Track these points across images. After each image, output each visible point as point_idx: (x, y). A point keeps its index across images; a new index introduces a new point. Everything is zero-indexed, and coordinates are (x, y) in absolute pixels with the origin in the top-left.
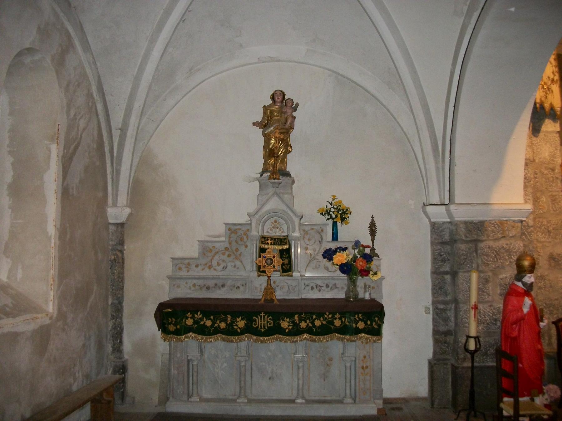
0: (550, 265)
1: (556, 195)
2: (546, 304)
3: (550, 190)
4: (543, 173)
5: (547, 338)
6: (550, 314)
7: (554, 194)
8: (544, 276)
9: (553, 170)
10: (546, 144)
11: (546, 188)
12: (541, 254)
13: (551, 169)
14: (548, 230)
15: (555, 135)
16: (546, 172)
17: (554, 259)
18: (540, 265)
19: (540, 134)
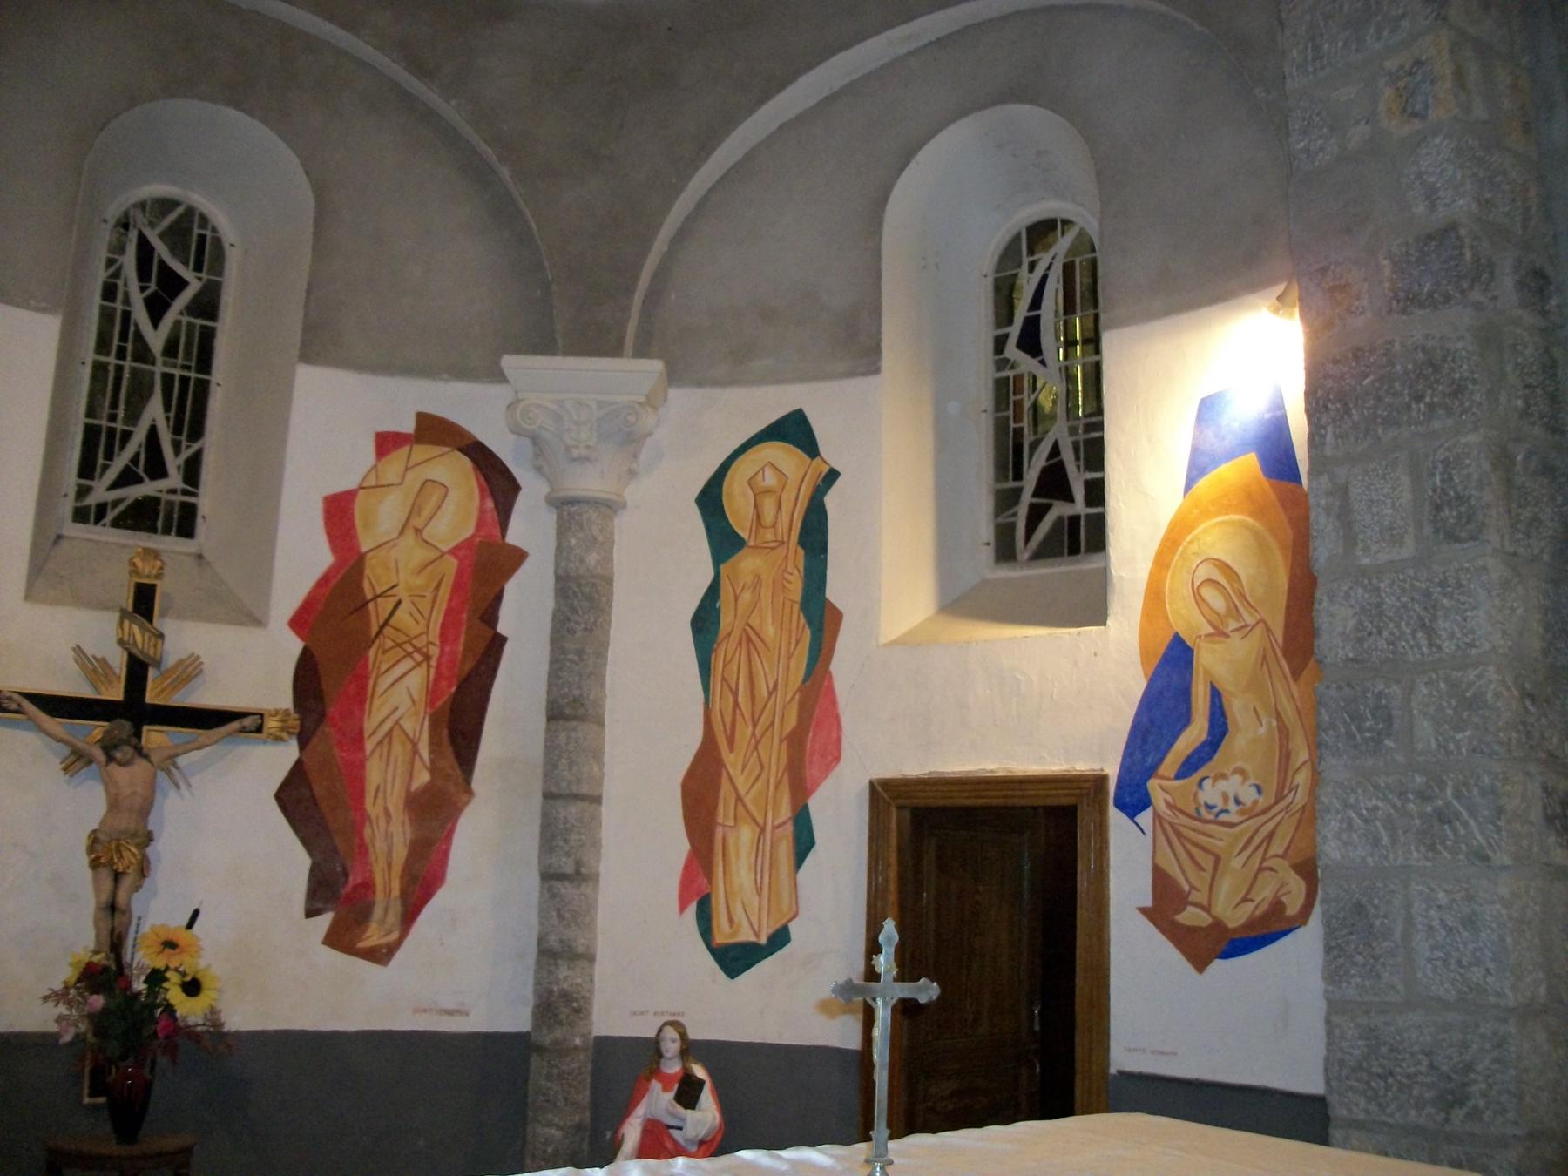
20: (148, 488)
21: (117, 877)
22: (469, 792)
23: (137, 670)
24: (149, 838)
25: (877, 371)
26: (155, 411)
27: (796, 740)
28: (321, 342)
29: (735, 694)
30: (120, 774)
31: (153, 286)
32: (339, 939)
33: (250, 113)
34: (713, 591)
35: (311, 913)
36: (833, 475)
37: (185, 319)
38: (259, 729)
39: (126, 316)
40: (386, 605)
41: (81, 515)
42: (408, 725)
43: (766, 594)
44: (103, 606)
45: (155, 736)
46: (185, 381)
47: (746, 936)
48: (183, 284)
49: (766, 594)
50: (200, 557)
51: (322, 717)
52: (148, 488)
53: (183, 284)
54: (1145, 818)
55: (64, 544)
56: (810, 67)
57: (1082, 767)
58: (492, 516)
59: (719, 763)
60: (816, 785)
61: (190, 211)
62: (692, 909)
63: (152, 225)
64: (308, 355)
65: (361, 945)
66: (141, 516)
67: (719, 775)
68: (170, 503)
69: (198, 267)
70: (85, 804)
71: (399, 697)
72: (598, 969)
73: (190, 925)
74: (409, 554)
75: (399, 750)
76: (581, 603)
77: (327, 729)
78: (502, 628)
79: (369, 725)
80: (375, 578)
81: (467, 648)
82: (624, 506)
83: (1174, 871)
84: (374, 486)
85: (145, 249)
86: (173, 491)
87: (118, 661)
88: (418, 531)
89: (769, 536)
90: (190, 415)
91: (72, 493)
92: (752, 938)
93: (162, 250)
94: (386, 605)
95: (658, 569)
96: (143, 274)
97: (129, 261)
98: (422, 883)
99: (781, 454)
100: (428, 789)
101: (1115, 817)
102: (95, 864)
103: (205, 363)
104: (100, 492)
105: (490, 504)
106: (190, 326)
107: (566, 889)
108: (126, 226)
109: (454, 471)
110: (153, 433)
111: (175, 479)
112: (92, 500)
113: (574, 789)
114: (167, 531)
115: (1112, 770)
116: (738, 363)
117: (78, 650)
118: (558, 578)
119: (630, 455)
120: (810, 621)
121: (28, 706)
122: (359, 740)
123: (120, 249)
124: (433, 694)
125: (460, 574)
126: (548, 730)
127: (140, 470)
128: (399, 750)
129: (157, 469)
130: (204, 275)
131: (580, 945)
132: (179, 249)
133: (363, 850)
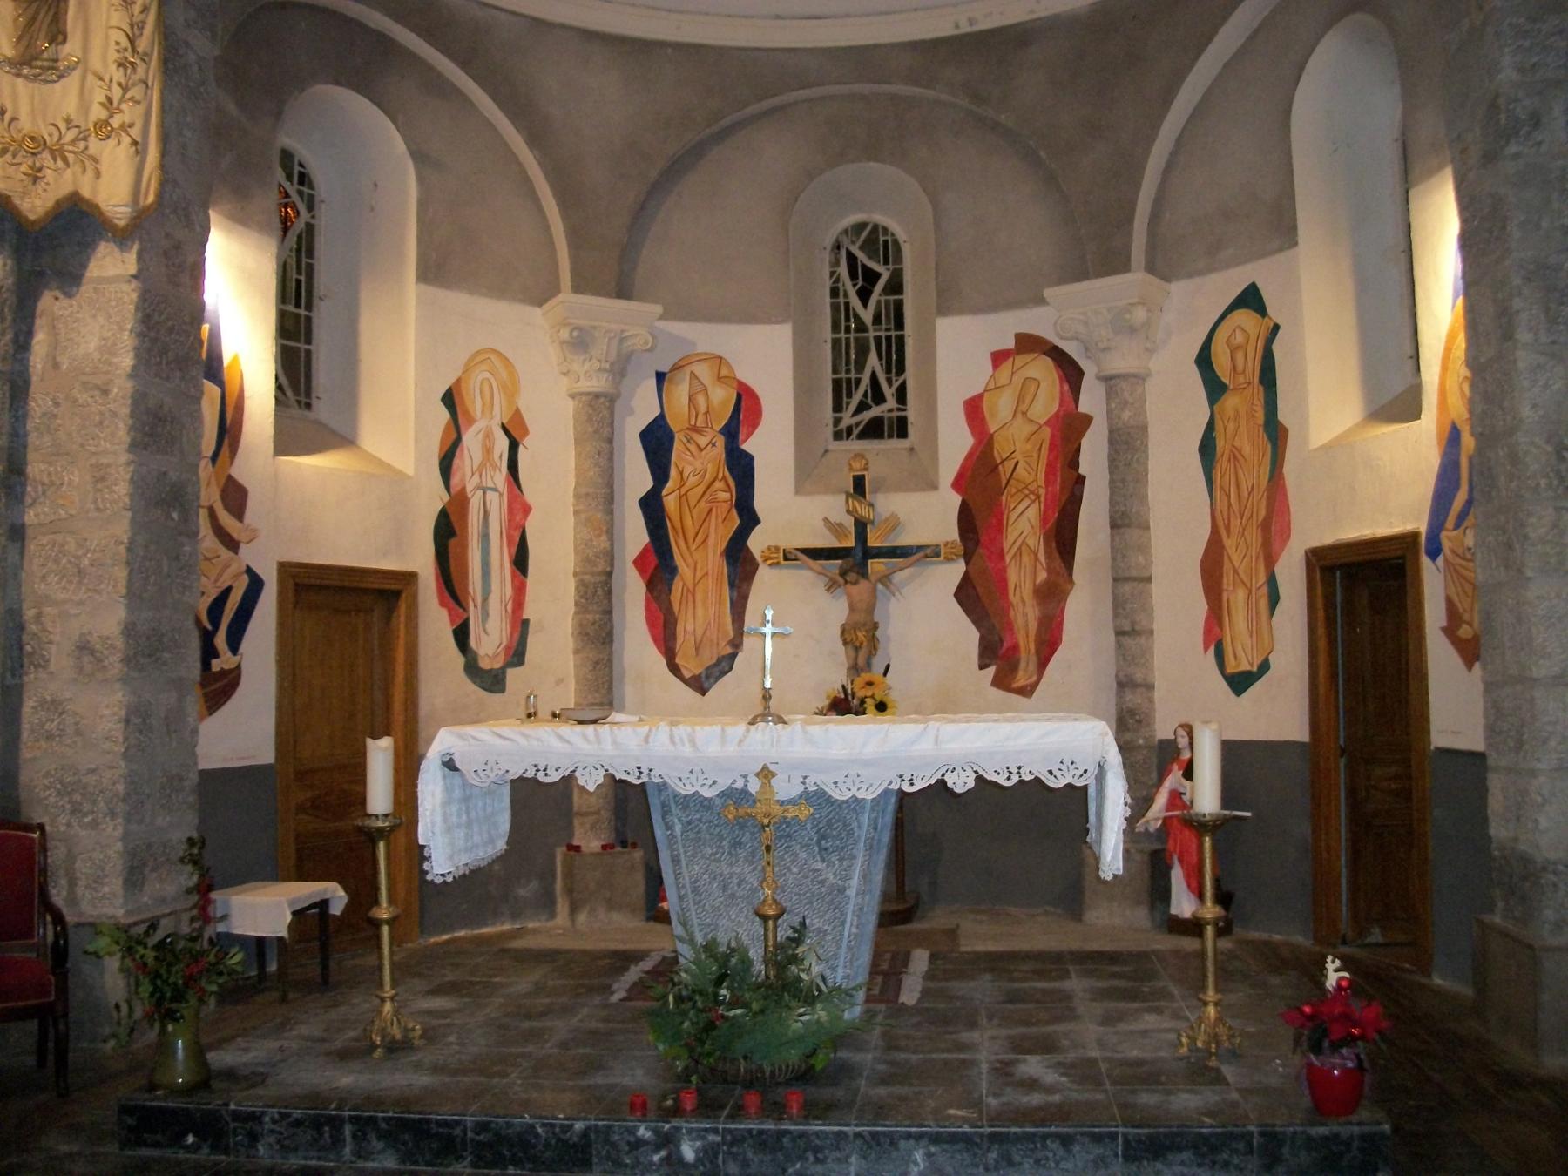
0: (81, 669)
1: (108, 465)
2: (61, 783)
3: (93, 449)
4: (75, 401)
5: (63, 882)
6: (73, 812)
7: (105, 461)
8: (61, 703)
9: (105, 392)
10: (94, 316)
11: (82, 445)
12: (57, 638)
13: (98, 387)
14: (78, 566)
15: (126, 287)
16: (83, 397)
17: (92, 652)
18: (52, 667)
19: (83, 289)
20: (875, 411)
21: (857, 649)
22: (1071, 581)
23: (861, 526)
24: (875, 626)
25: (1296, 244)
26: (873, 361)
27: (1265, 526)
28: (948, 302)
29: (1229, 496)
30: (854, 589)
31: (860, 283)
32: (1001, 682)
33: (883, 161)
34: (1211, 426)
35: (982, 667)
36: (1276, 327)
37: (883, 298)
38: (938, 555)
39: (847, 305)
40: (1009, 465)
41: (838, 436)
42: (1031, 542)
43: (1243, 422)
44: (839, 491)
45: (876, 566)
46: (888, 338)
47: (1245, 667)
48: (878, 276)
49: (1243, 422)
50: (912, 449)
51: (977, 543)
52: (875, 411)
53: (878, 276)
54: (1440, 560)
55: (829, 456)
56: (1225, 19)
57: (1409, 527)
58: (1069, 397)
59: (1223, 547)
60: (1278, 555)
61: (876, 227)
62: (1212, 650)
63: (853, 243)
64: (944, 310)
65: (1015, 685)
66: (874, 430)
67: (1222, 556)
68: (890, 419)
69: (886, 262)
70: (836, 610)
71: (1024, 524)
72: (1157, 695)
73: (885, 674)
74: (1021, 430)
75: (1026, 559)
76: (1127, 447)
77: (980, 550)
78: (1082, 471)
79: (1006, 546)
80: (1001, 450)
81: (1062, 488)
82: (1149, 375)
83: (1456, 599)
84: (994, 388)
85: (852, 259)
86: (890, 411)
87: (849, 522)
88: (1024, 414)
89: (1242, 379)
90: (895, 360)
91: (831, 422)
92: (1248, 668)
93: (862, 257)
94: (1009, 465)
95: (1175, 414)
96: (853, 276)
97: (843, 270)
98: (1049, 642)
99: (1244, 317)
100: (1047, 582)
101: (1425, 561)
102: (845, 643)
103: (900, 324)
104: (847, 420)
105: (1066, 387)
106: (887, 302)
107: (1127, 641)
108: (838, 248)
109: (1042, 370)
110: (874, 376)
111: (891, 402)
112: (843, 425)
113: (1127, 574)
114: (890, 436)
115: (1423, 527)
116: (1213, 258)
117: (826, 520)
118: (1110, 432)
119: (1150, 337)
120: (1270, 438)
121: (801, 555)
122: (1001, 556)
123: (837, 263)
124: (1044, 520)
125: (1053, 436)
126: (1112, 536)
127: (869, 401)
128: (1026, 559)
129: (879, 398)
130: (891, 266)
131: (1139, 676)
132: (873, 255)
133: (1010, 626)
